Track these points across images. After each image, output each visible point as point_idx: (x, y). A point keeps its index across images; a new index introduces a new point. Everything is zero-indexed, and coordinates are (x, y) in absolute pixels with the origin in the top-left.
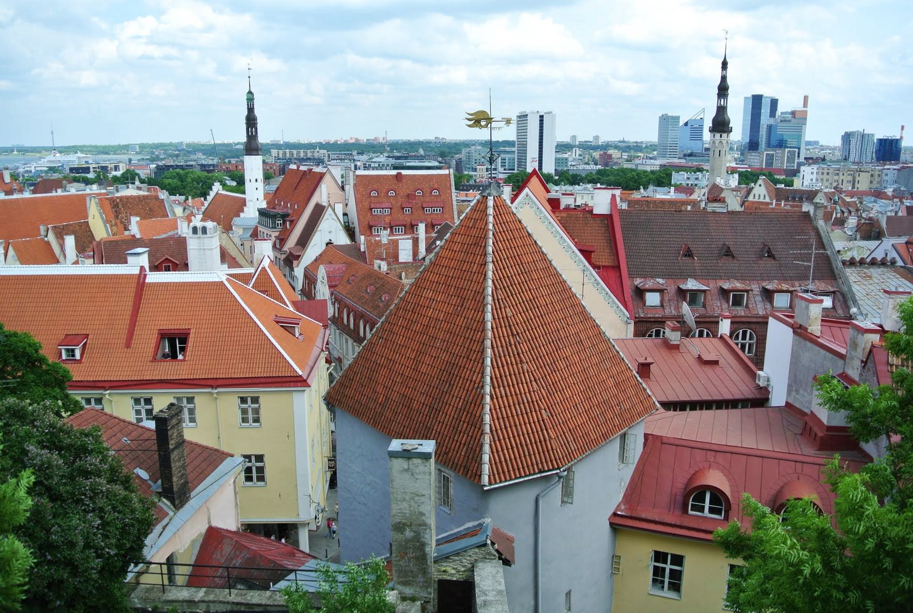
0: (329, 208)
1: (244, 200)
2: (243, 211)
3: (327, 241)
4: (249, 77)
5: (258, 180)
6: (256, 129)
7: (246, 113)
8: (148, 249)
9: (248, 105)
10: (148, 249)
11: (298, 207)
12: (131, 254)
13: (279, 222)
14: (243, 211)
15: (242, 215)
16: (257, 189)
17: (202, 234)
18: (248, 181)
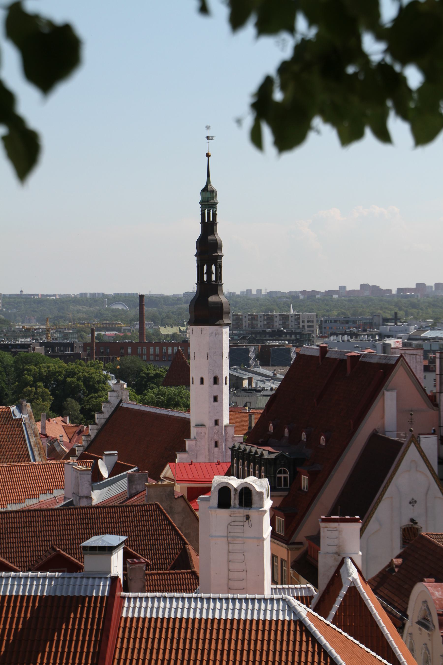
0: (413, 447)
1: (186, 423)
2: (183, 450)
3: (406, 522)
4: (208, 155)
5: (220, 381)
6: (220, 267)
7: (197, 232)
8: (123, 538)
9: (203, 215)
10: (123, 538)
11: (327, 440)
12: (93, 549)
13: (282, 476)
14: (183, 450)
15: (180, 457)
16: (216, 399)
17: (241, 504)
18: (197, 381)
